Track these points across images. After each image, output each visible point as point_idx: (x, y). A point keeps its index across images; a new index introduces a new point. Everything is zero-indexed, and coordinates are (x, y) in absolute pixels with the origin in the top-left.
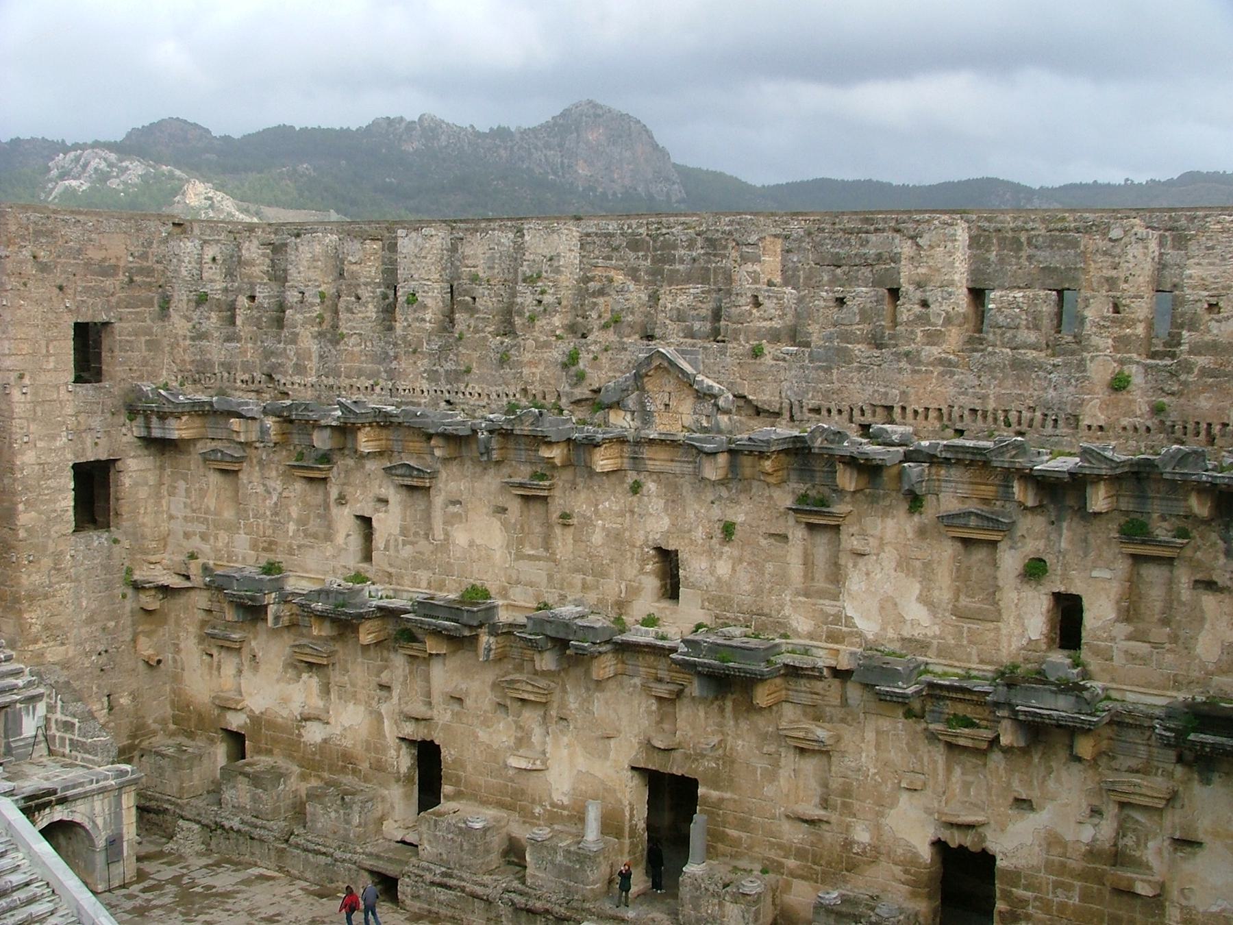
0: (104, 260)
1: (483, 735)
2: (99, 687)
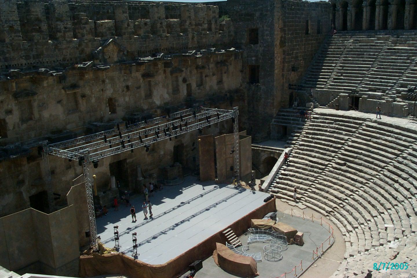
1: (64, 179)
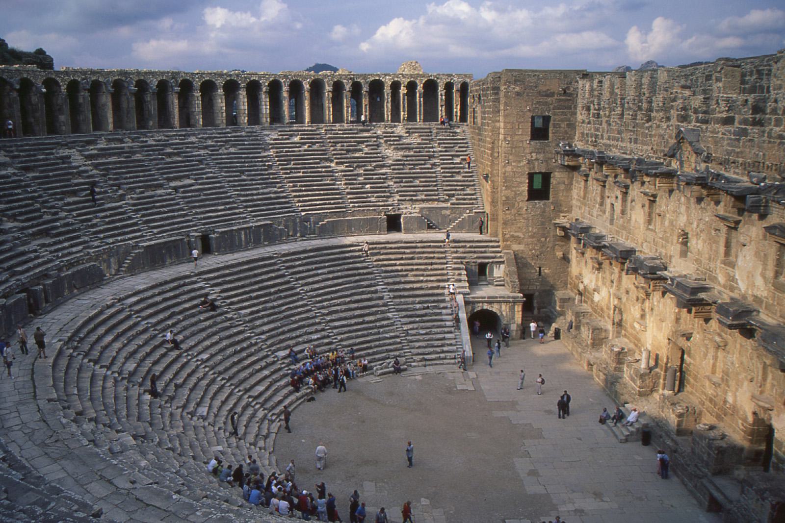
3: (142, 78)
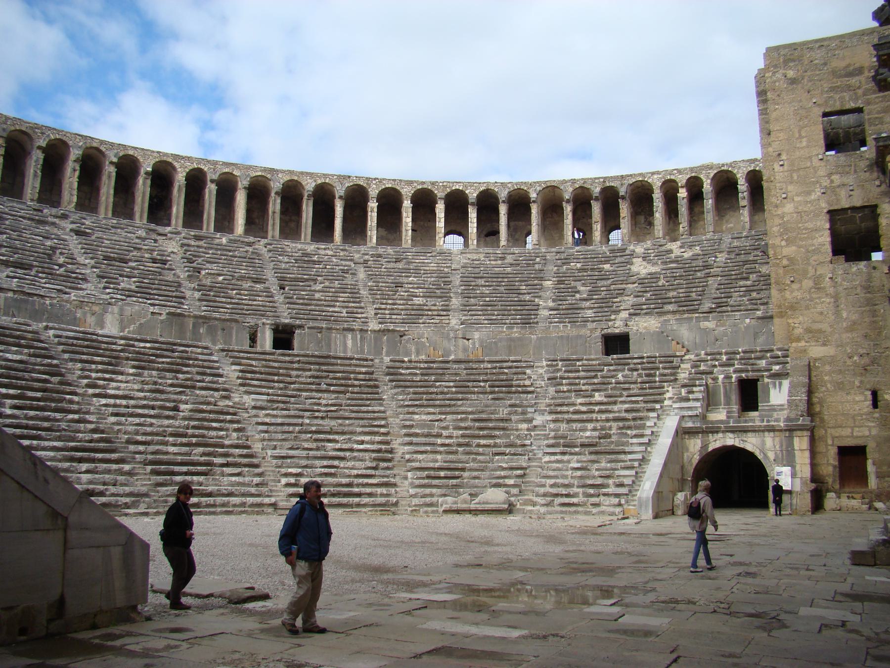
0: (849, 66)
2: (861, 382)
3: (296, 178)
